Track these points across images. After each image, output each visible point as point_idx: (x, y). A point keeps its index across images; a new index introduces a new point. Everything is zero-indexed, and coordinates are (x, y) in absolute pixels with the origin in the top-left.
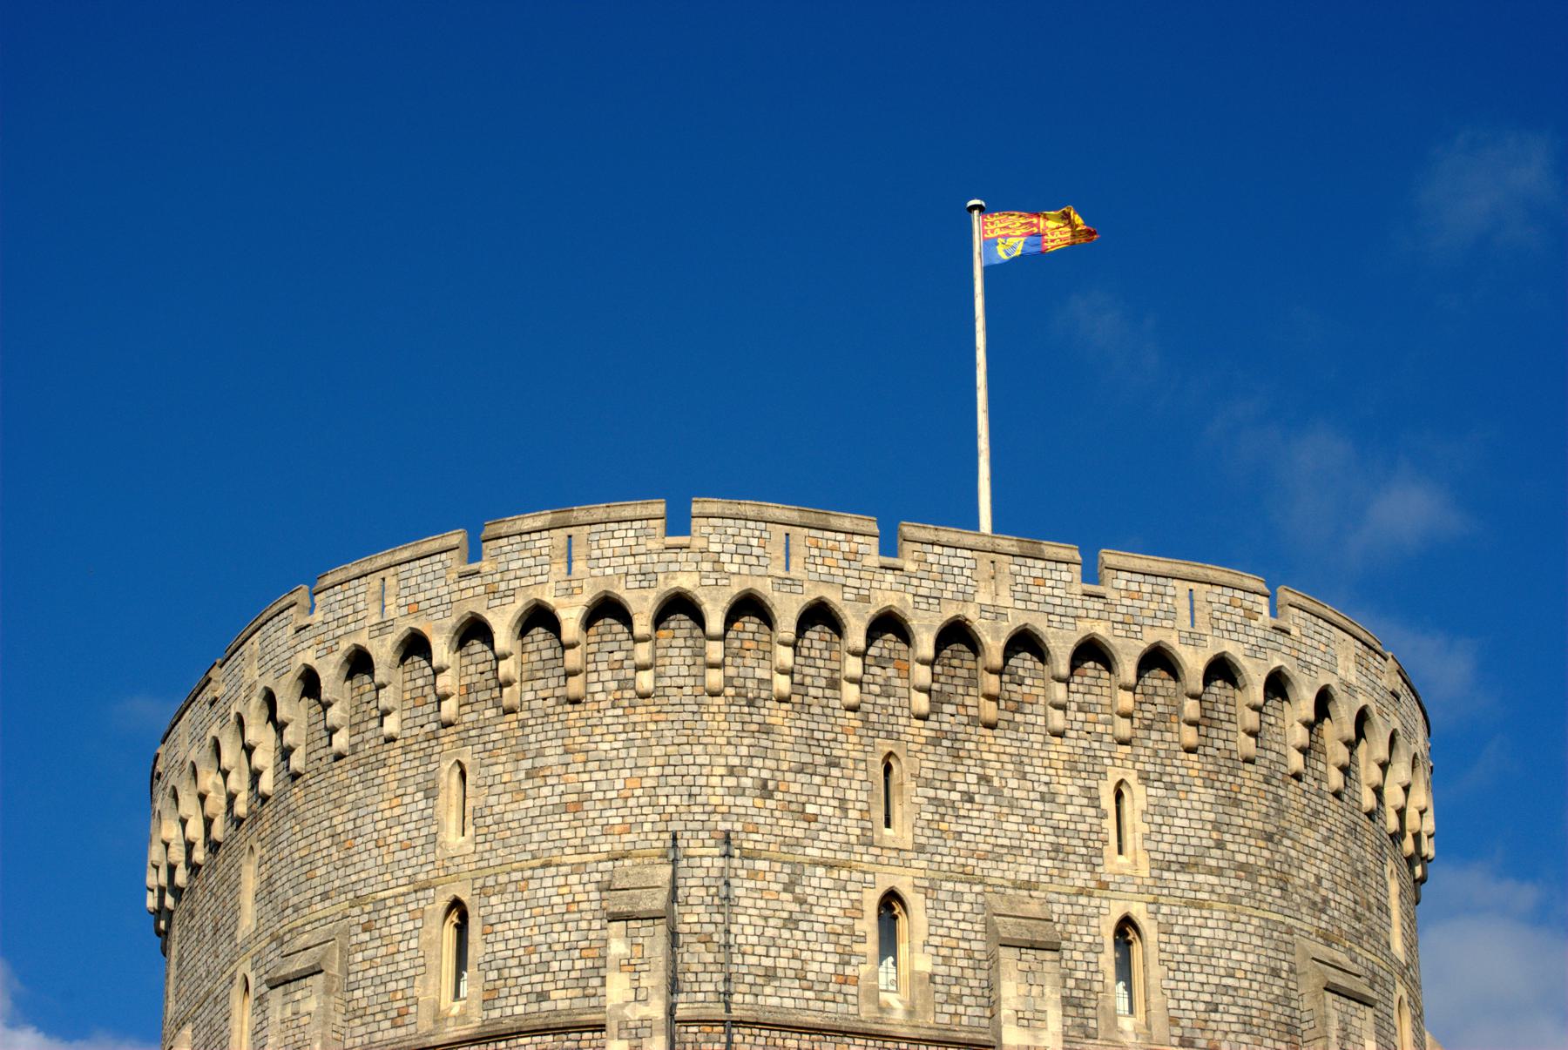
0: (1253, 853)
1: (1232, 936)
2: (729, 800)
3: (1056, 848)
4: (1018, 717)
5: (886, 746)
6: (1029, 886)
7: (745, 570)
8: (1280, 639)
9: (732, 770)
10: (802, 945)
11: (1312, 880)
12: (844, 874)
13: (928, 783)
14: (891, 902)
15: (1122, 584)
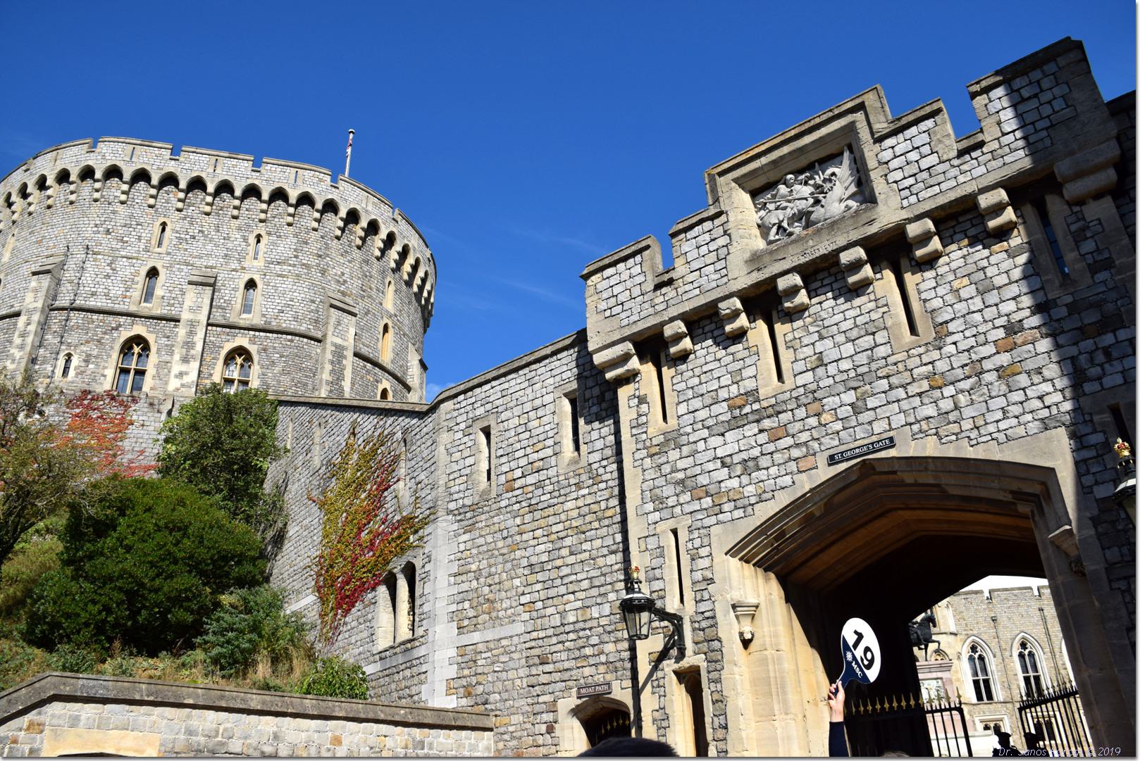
0: (313, 261)
1: (295, 287)
2: (93, 235)
3: (226, 255)
4: (220, 212)
5: (162, 220)
6: (211, 267)
7: (114, 158)
8: (334, 190)
9: (96, 226)
10: (111, 284)
11: (339, 273)
12: (134, 261)
13: (177, 232)
14: (153, 273)
15: (269, 168)
